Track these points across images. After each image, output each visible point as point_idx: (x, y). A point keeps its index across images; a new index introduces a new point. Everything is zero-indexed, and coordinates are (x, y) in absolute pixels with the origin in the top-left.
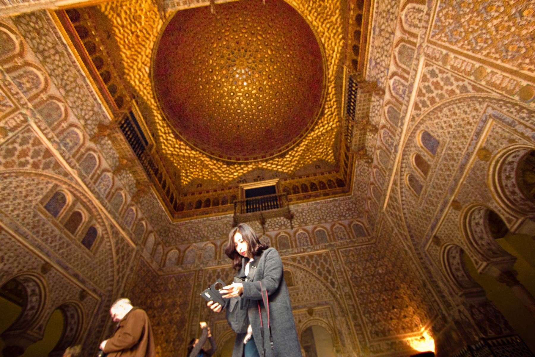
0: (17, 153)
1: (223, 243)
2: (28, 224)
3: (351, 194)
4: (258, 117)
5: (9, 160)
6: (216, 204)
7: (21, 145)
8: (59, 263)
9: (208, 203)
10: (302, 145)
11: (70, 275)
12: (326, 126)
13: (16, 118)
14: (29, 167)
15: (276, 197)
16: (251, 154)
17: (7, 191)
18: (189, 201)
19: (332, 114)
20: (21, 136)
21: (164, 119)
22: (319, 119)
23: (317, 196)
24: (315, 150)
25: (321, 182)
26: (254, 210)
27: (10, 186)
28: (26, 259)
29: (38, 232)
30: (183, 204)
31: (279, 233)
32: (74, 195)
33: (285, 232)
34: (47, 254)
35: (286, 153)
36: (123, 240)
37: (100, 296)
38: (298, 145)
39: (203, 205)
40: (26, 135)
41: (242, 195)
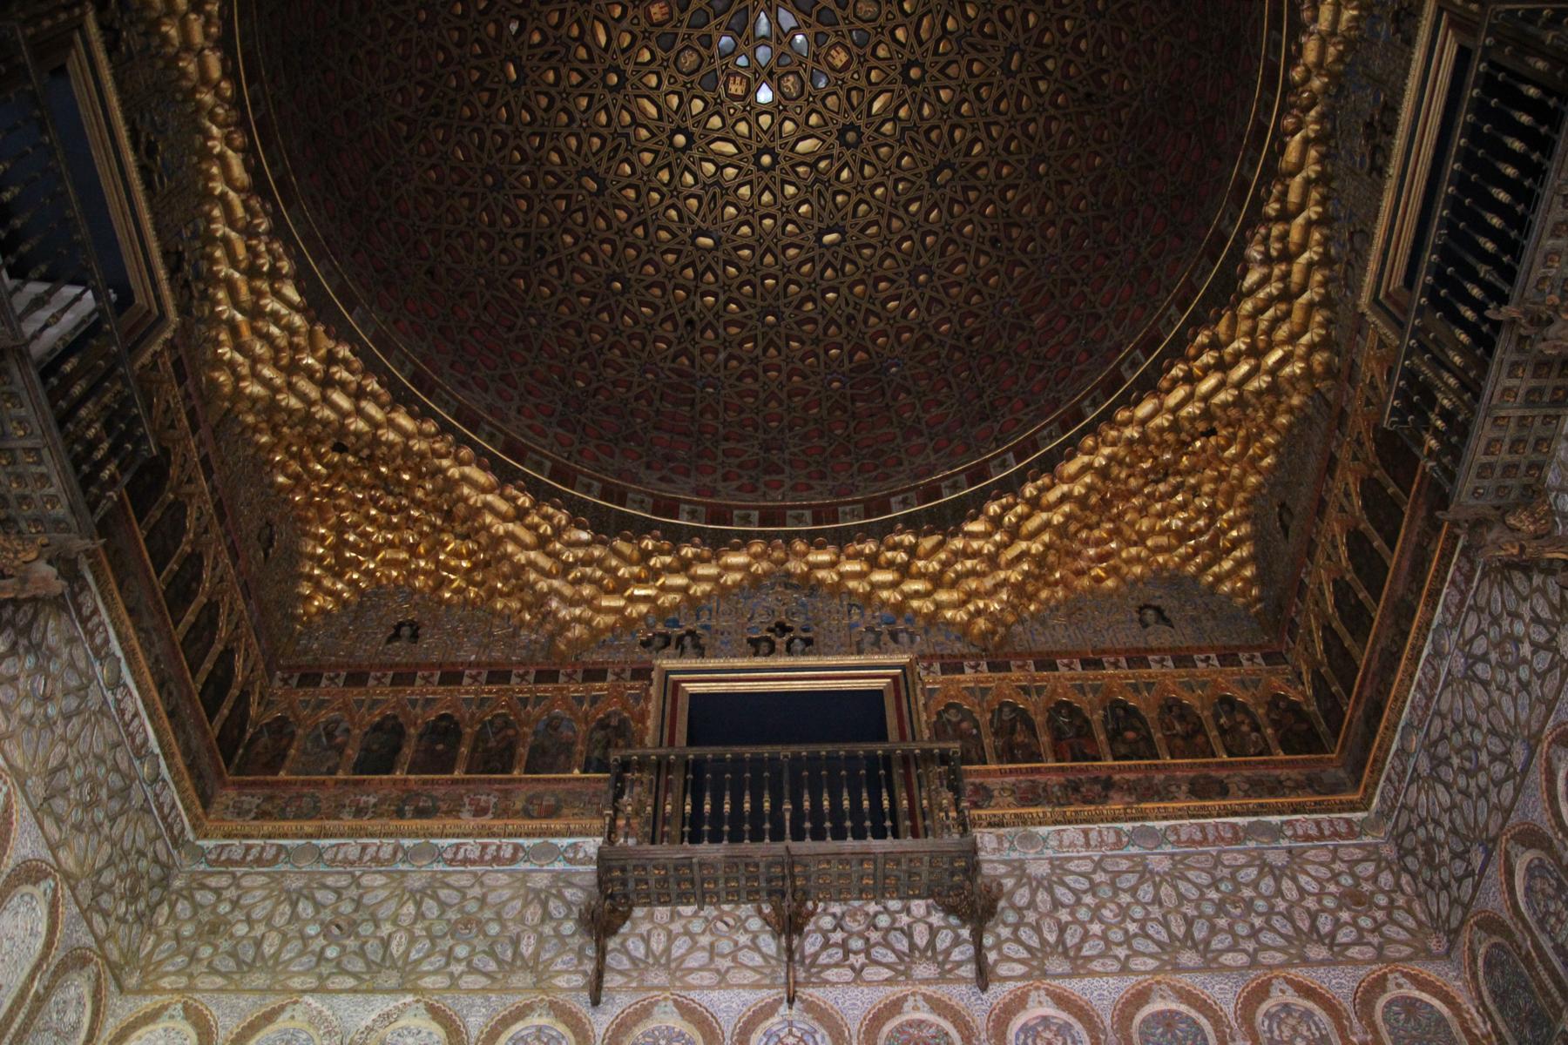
1: (506, 1022)
3: (1364, 805)
4: (814, 292)
6: (495, 758)
9: (441, 744)
10: (1072, 467)
12: (1244, 368)
15: (887, 760)
16: (754, 489)
18: (324, 716)
19: (1287, 296)
21: (258, 187)
22: (1197, 322)
23: (1148, 791)
24: (1143, 511)
25: (1174, 709)
26: (738, 829)
30: (281, 729)
31: (895, 1007)
33: (937, 1006)
35: (973, 508)
38: (1049, 465)
39: (408, 752)
41: (668, 720)
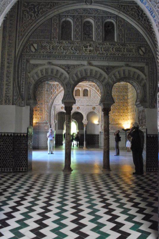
0: (53, 92)
5: (52, 94)
8: (80, 105)
14: (57, 92)
40: (51, 86)
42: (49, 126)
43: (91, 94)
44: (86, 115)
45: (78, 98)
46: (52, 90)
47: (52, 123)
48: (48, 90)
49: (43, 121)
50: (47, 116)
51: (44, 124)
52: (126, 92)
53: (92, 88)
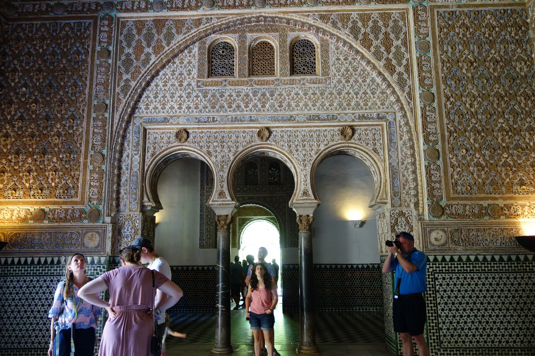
0: (133, 57)
2: (205, 107)
5: (132, 69)
7: (129, 45)
11: (304, 122)
13: (102, 29)
14: (153, 58)
17: (160, 96)
20: (122, 38)
27: (159, 88)
28: (234, 138)
29: (222, 107)
32: (234, 32)
34: (251, 120)
36: (365, 18)
37: (379, 118)
40: (125, 31)
42: (110, 228)
43: (332, 59)
44: (309, 168)
45: (267, 83)
46: (131, 51)
47: (125, 211)
48: (111, 48)
49: (76, 203)
50: (100, 179)
51: (80, 219)
52: (519, 43)
53: (335, 31)
